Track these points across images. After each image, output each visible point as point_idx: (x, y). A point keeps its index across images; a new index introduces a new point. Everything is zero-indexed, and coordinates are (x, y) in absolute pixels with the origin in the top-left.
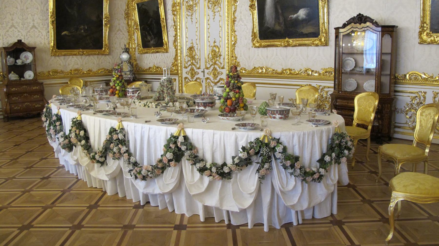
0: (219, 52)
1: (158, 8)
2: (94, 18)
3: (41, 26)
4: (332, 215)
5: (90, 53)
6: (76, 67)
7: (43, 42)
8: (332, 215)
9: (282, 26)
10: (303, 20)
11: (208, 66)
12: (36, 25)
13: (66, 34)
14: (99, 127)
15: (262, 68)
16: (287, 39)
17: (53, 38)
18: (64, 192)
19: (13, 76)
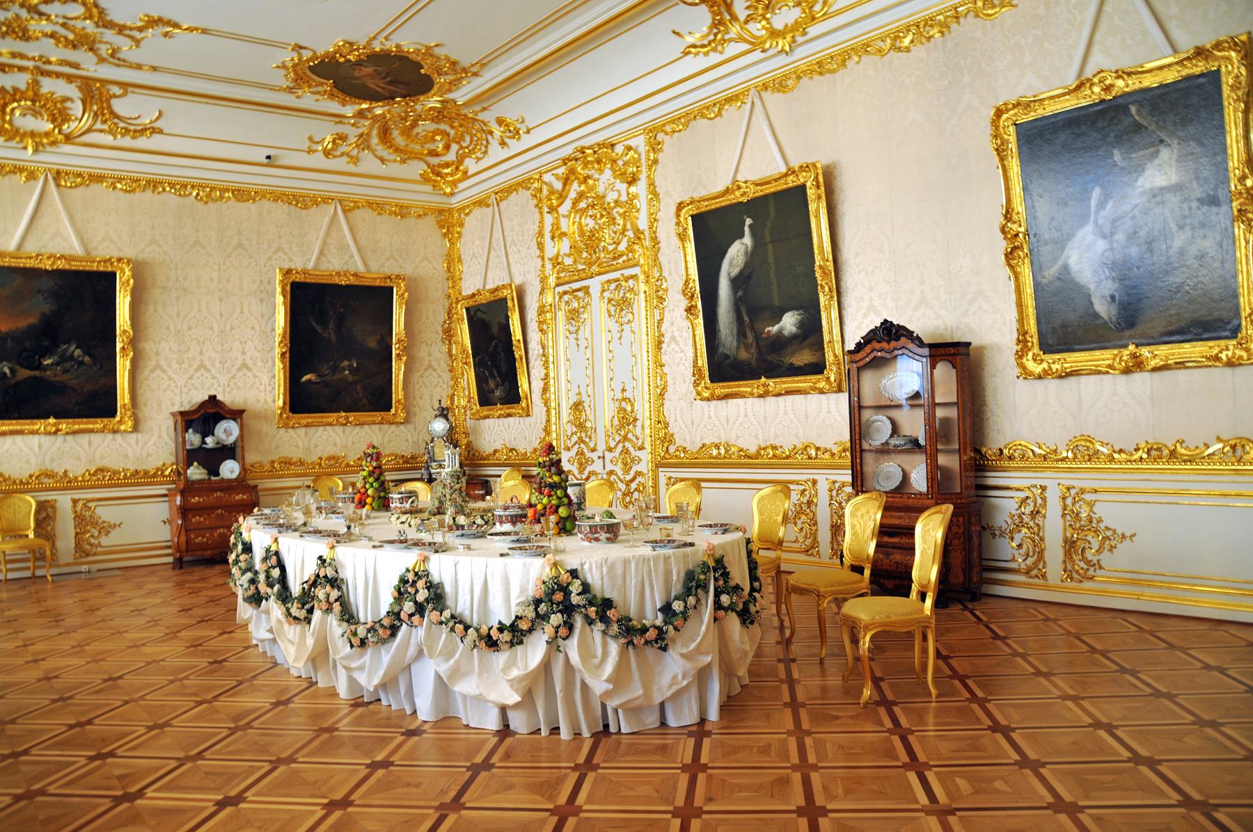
0: (632, 411)
1: (507, 318)
2: (372, 343)
3: (260, 364)
4: (703, 721)
5: (363, 419)
6: (331, 451)
7: (262, 396)
8: (703, 721)
9: (753, 350)
10: (794, 337)
11: (612, 444)
12: (249, 362)
13: (309, 381)
14: (302, 559)
15: (717, 447)
16: (763, 379)
17: (282, 390)
18: (240, 683)
19: (196, 472)
